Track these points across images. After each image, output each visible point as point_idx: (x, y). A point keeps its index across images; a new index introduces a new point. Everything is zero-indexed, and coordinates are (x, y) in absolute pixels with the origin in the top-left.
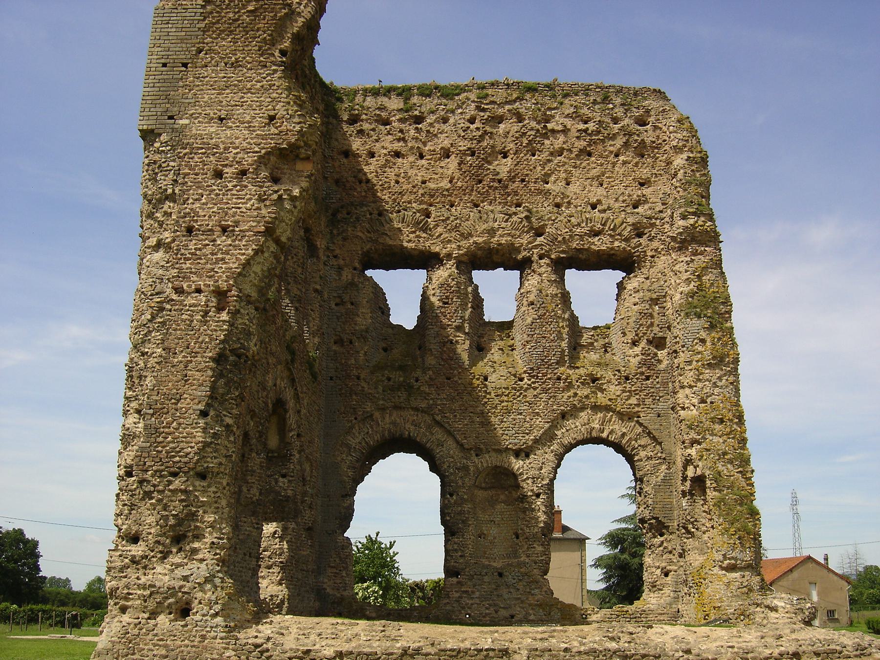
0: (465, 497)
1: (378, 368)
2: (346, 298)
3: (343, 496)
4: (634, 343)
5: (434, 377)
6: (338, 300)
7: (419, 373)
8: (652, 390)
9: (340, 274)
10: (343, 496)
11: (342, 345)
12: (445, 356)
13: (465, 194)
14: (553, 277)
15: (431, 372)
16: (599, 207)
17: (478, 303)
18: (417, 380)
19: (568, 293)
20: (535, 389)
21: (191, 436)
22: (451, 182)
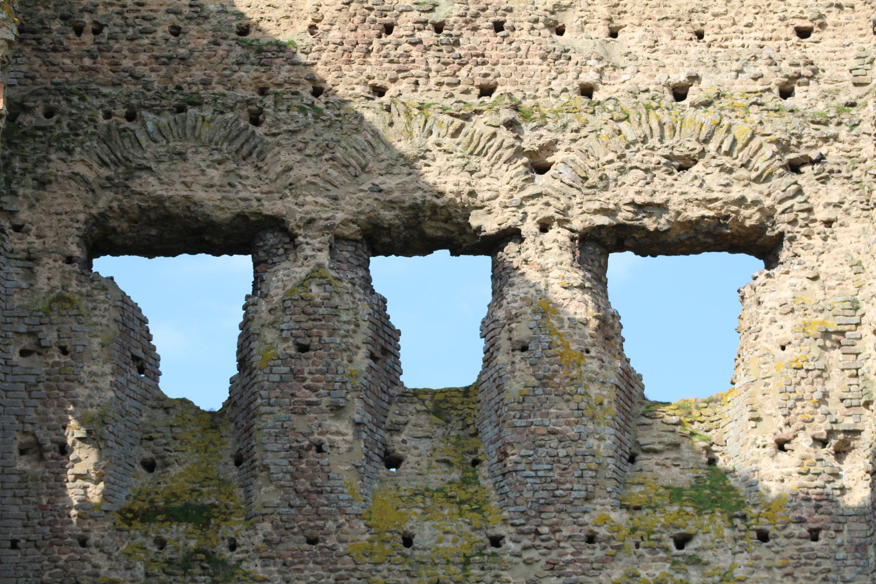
1: (130, 516)
2: (50, 336)
4: (781, 445)
5: (275, 537)
6: (27, 342)
7: (236, 527)
8: (827, 564)
9: (30, 273)
11: (41, 458)
12: (304, 484)
13: (349, 62)
14: (577, 277)
15: (267, 526)
16: (694, 94)
17: (385, 343)
18: (233, 547)
19: (616, 316)
20: (528, 563)
22: (312, 29)
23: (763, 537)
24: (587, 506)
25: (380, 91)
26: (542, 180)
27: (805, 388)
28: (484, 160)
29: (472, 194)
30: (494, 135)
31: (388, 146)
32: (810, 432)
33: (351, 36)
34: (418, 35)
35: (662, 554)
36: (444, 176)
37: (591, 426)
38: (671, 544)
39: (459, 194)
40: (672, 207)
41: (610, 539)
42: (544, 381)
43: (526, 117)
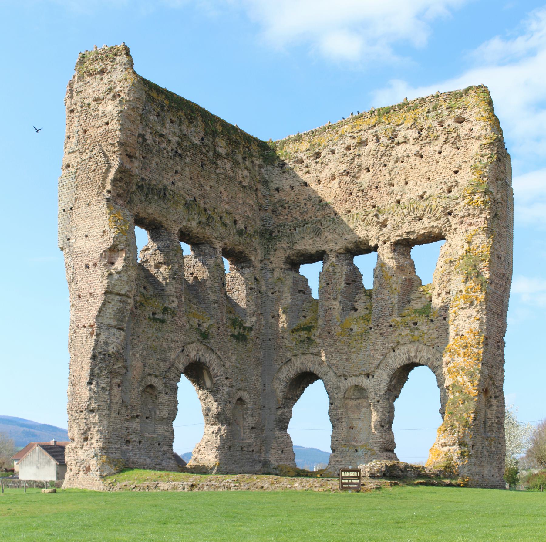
0: (339, 405)
3: (277, 409)
10: (277, 409)
13: (342, 205)
14: (391, 255)
21: (85, 393)
23: (432, 321)
24: (390, 317)
25: (349, 211)
26: (384, 230)
27: (445, 278)
28: (370, 227)
29: (368, 236)
30: (372, 219)
31: (348, 227)
32: (445, 290)
33: (342, 198)
34: (358, 194)
35: (408, 328)
36: (361, 233)
37: (392, 296)
38: (412, 325)
39: (364, 237)
40: (416, 231)
41: (395, 326)
42: (380, 285)
43: (380, 213)
